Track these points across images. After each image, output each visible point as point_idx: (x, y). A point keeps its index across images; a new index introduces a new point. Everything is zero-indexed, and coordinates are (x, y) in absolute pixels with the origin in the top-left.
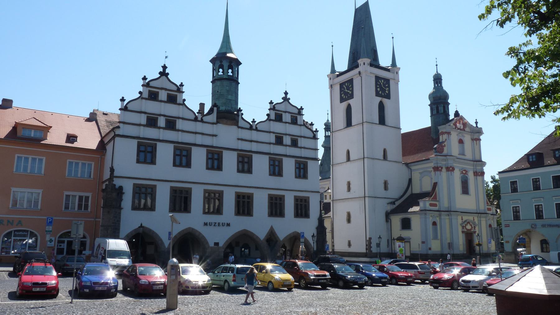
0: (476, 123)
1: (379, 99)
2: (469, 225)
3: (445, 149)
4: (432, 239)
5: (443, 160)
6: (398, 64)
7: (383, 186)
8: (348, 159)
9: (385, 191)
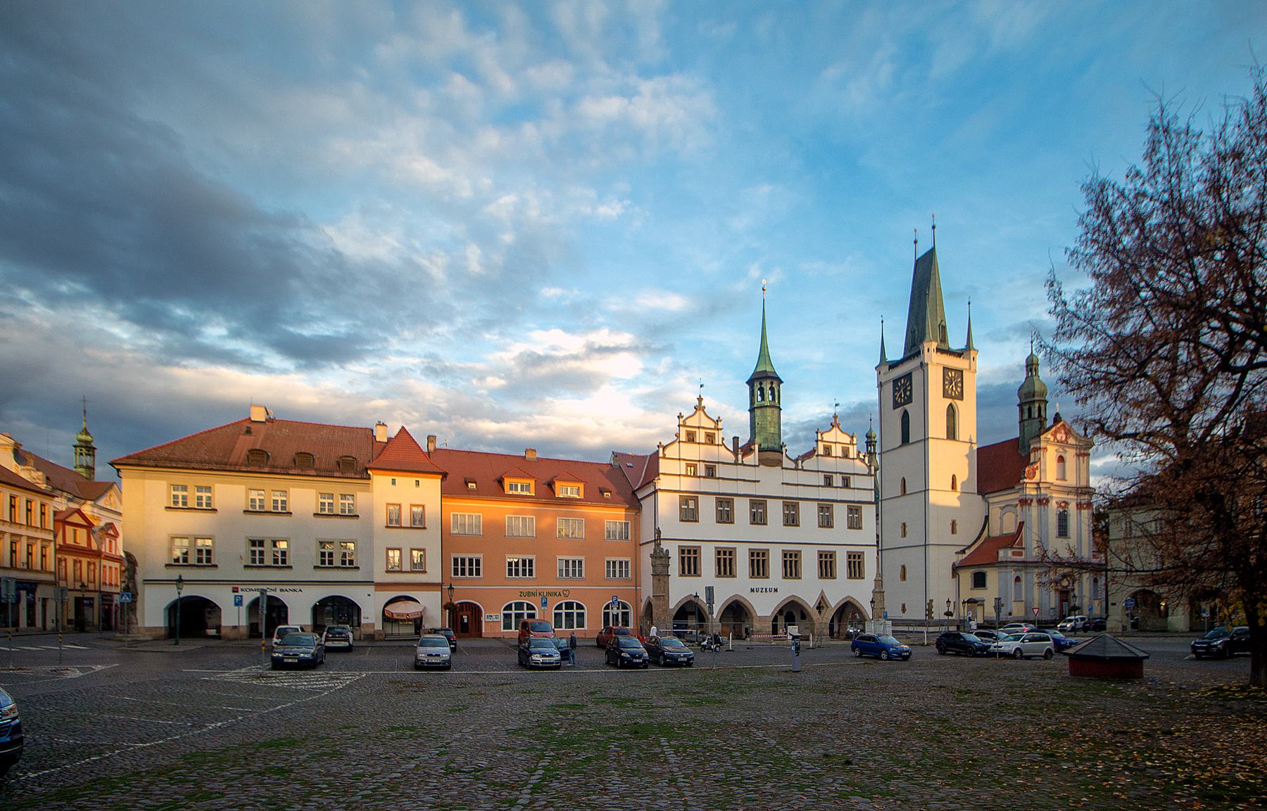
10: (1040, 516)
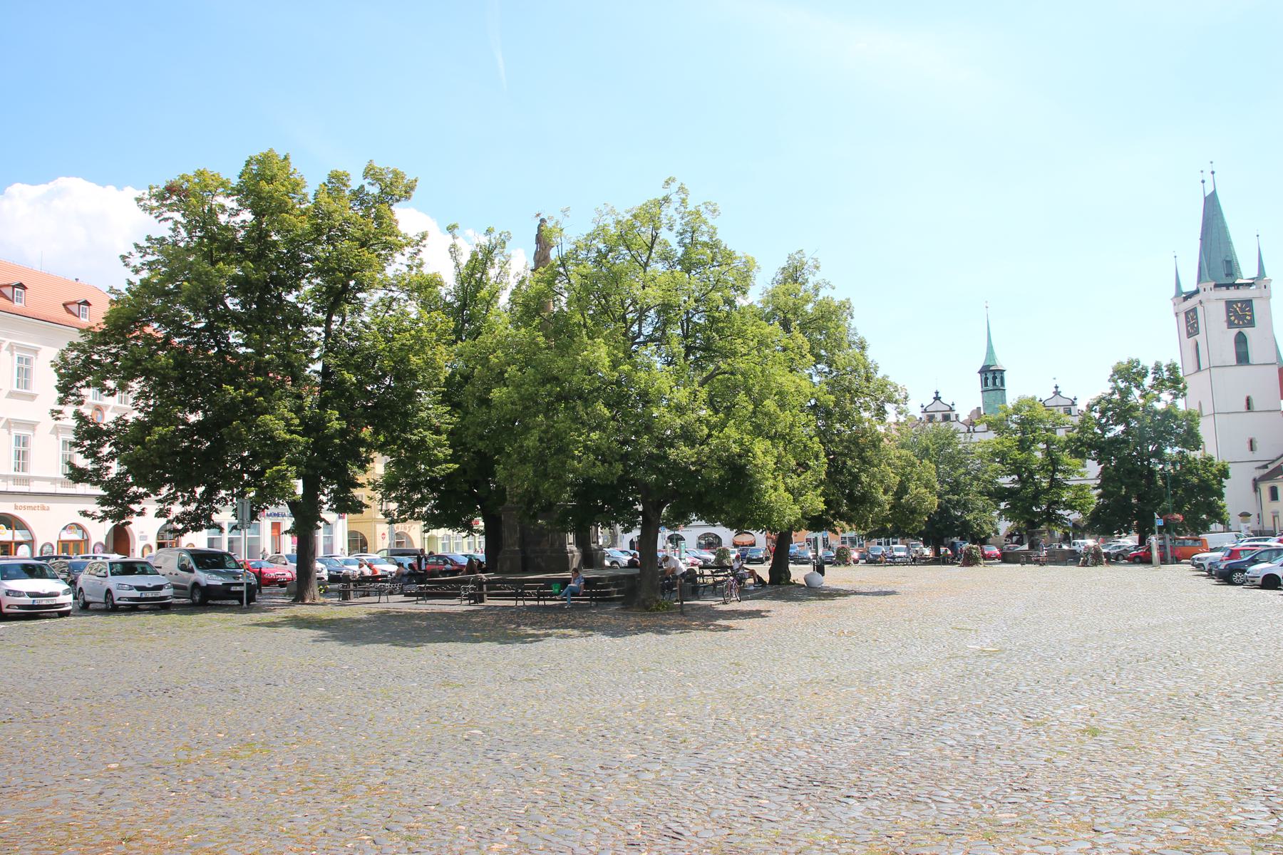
1: (1237, 330)
6: (1269, 273)
7: (1247, 446)
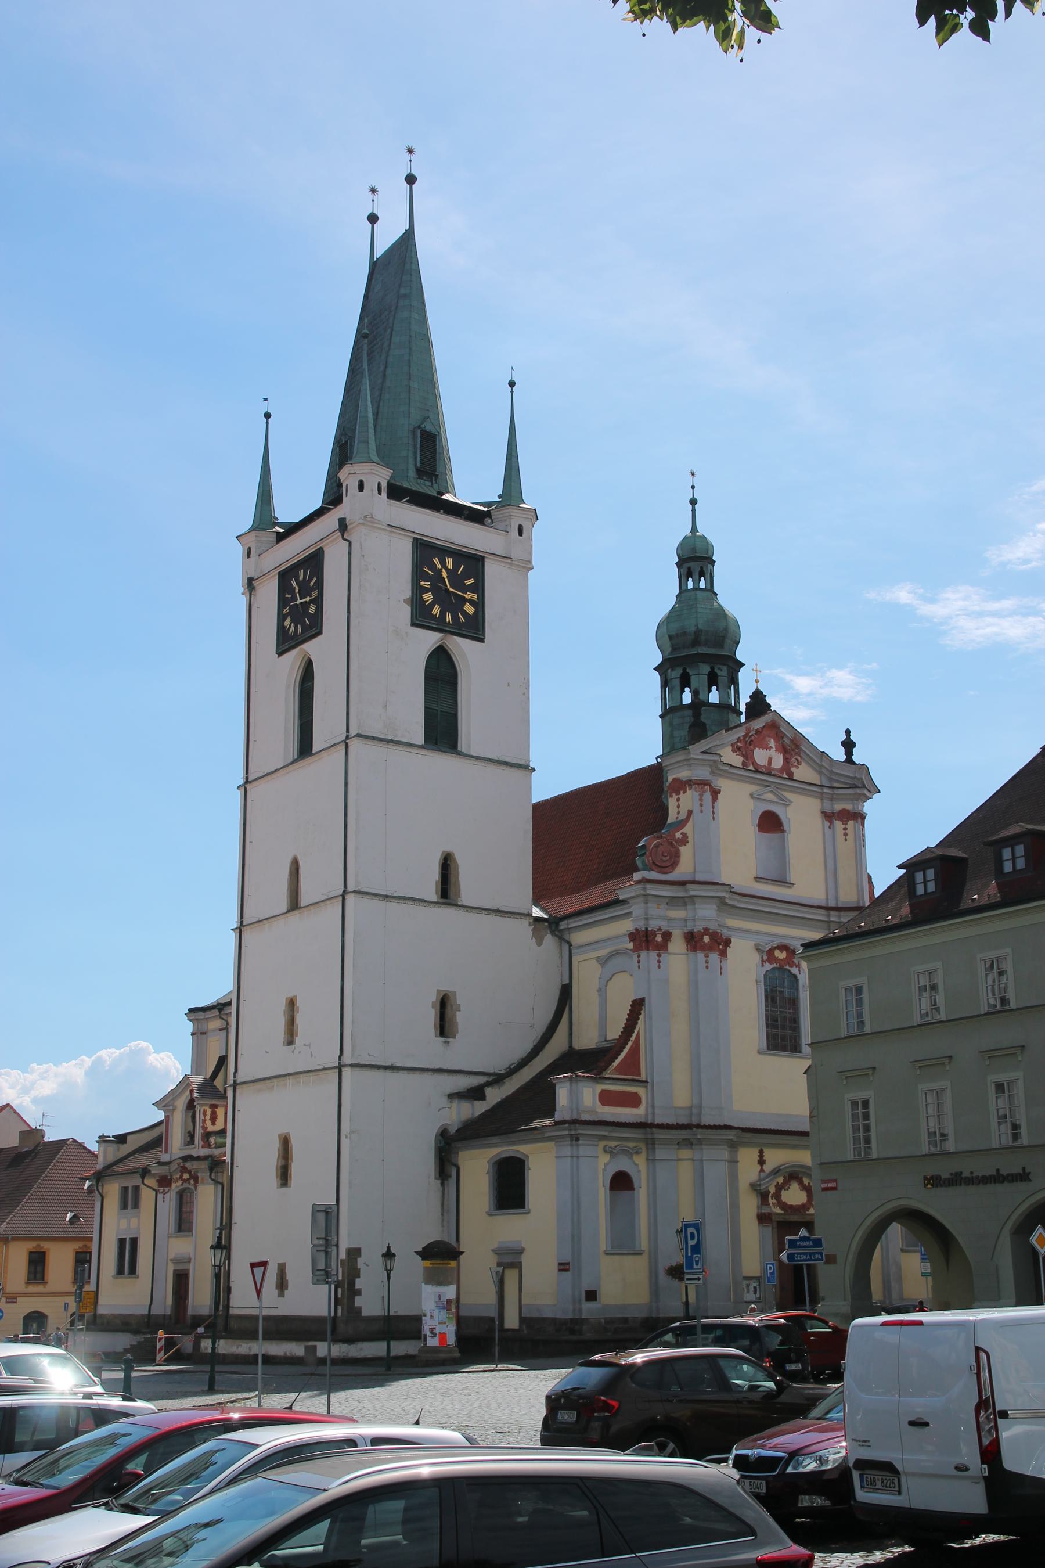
0: (849, 745)
1: (430, 639)
2: (795, 1186)
3: (685, 851)
4: (607, 1253)
5: (673, 902)
7: (431, 1016)
8: (294, 904)
9: (443, 1039)
10: (694, 985)
